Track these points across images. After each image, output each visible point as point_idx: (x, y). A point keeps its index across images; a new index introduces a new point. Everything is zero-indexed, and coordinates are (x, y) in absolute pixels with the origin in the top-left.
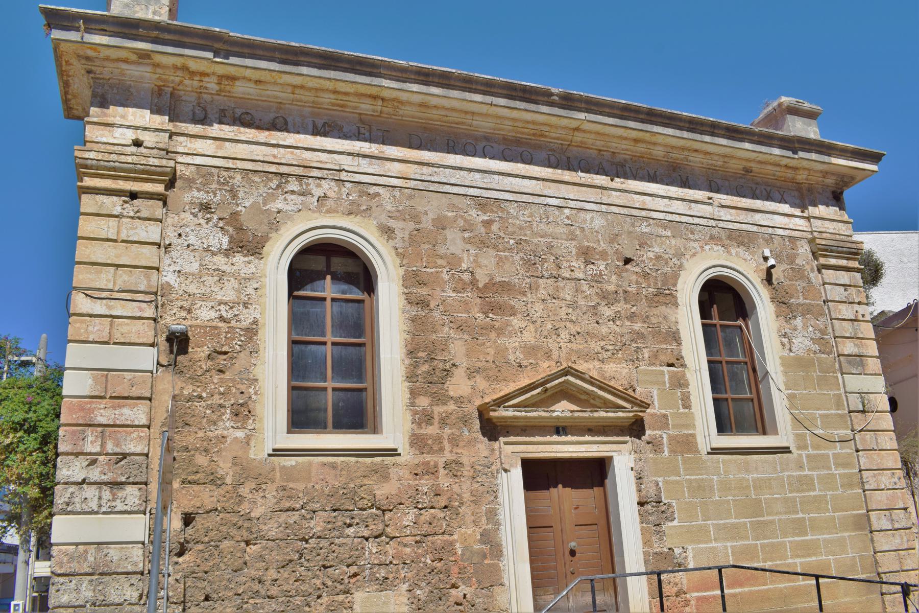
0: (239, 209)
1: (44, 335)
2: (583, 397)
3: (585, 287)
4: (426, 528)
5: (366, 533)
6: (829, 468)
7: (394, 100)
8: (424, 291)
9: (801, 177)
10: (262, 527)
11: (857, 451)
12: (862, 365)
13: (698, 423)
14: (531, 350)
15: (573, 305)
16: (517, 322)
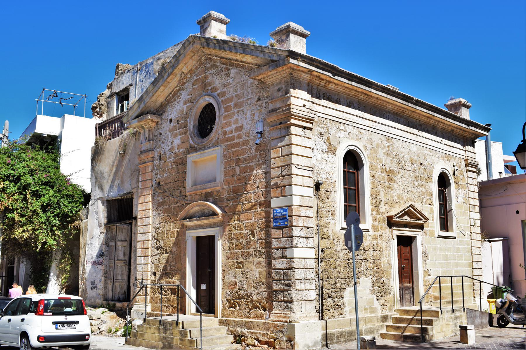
0: (330, 135)
1: (7, 122)
2: (411, 215)
4: (375, 258)
5: (362, 258)
6: (464, 245)
7: (370, 96)
8: (374, 172)
9: (466, 134)
10: (339, 254)
12: (475, 208)
13: (435, 226)
14: (399, 196)
15: (408, 180)
16: (395, 186)
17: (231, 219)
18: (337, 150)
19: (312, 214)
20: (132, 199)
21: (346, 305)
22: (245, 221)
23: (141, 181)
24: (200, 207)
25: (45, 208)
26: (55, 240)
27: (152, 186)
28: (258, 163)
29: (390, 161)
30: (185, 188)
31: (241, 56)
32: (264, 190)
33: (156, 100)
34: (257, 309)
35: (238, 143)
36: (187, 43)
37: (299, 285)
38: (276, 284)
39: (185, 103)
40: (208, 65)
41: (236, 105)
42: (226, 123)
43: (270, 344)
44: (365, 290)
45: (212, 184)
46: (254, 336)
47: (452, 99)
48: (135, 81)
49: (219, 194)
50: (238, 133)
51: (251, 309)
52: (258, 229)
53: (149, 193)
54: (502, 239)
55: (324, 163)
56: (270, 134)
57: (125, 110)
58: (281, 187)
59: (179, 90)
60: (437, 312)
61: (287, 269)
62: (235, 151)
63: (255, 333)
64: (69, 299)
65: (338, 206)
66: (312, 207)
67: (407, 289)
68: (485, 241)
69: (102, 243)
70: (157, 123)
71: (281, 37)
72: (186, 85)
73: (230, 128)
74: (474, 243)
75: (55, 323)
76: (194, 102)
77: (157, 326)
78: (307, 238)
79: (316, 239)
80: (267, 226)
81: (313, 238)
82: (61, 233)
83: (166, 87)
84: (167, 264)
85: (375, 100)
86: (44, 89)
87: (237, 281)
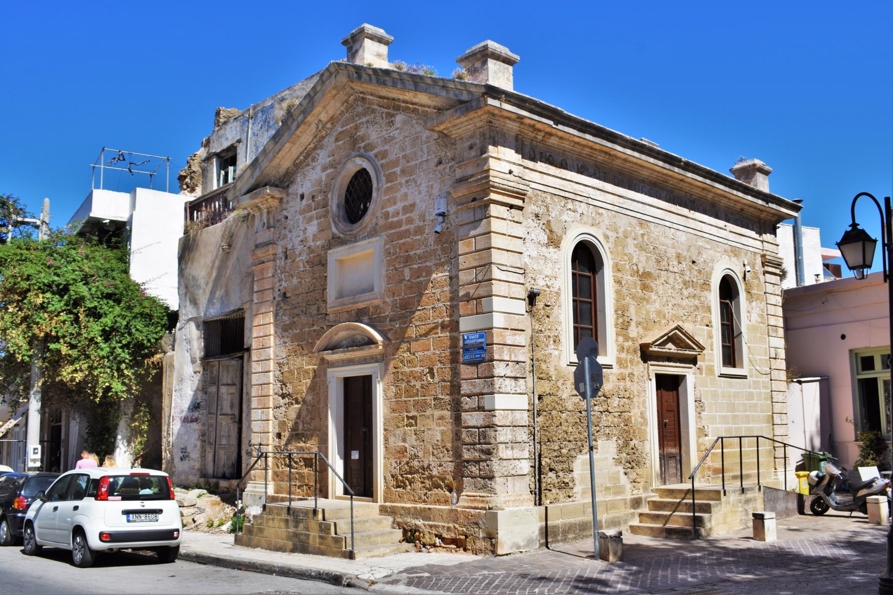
0: (550, 218)
1: (47, 200)
2: (677, 341)
3: (678, 278)
4: (622, 409)
5: (602, 410)
6: (760, 389)
8: (619, 275)
9: (763, 216)
11: (771, 380)
12: (776, 331)
14: (659, 313)
15: (673, 288)
16: (653, 296)
17: (398, 349)
18: (562, 242)
19: (524, 341)
20: (242, 320)
21: (577, 482)
22: (420, 353)
23: (256, 292)
24: (349, 332)
25: (107, 335)
26: (124, 384)
27: (274, 298)
28: (438, 262)
29: (645, 258)
30: (325, 301)
31: (411, 94)
32: (449, 303)
33: (279, 165)
34: (439, 489)
35: (408, 231)
36: (327, 74)
37: (504, 452)
38: (468, 450)
39: (324, 169)
40: (360, 109)
41: (403, 172)
42: (388, 199)
43: (459, 544)
44: (606, 458)
45: (367, 296)
46: (434, 532)
47: (741, 160)
48: (245, 135)
49: (379, 311)
50: (408, 215)
51: (430, 490)
52: (439, 365)
53: (268, 310)
54: (819, 378)
55: (542, 262)
56: (457, 217)
57: (230, 180)
58: (476, 299)
59: (315, 148)
60: (718, 492)
61: (485, 427)
62: (403, 244)
63: (436, 527)
64: (148, 475)
65: (564, 329)
66: (524, 331)
67: (671, 456)
68: (793, 381)
69: (197, 389)
70: (281, 200)
71: (474, 65)
72: (326, 140)
73: (395, 207)
74: (776, 386)
75: (127, 513)
76: (339, 167)
77: (284, 516)
78: (516, 378)
79: (530, 379)
80: (454, 360)
81: (525, 378)
82: (132, 373)
83: (294, 144)
84: (298, 421)
85: (622, 162)
86: (103, 149)
87: (407, 445)
